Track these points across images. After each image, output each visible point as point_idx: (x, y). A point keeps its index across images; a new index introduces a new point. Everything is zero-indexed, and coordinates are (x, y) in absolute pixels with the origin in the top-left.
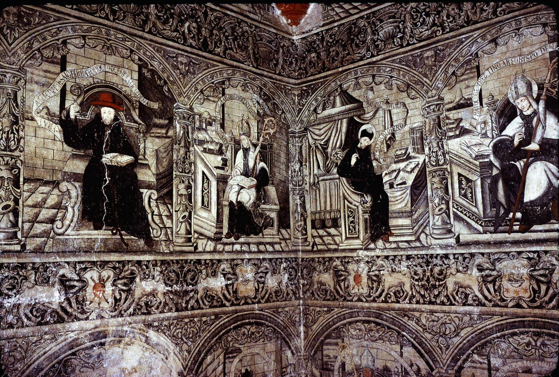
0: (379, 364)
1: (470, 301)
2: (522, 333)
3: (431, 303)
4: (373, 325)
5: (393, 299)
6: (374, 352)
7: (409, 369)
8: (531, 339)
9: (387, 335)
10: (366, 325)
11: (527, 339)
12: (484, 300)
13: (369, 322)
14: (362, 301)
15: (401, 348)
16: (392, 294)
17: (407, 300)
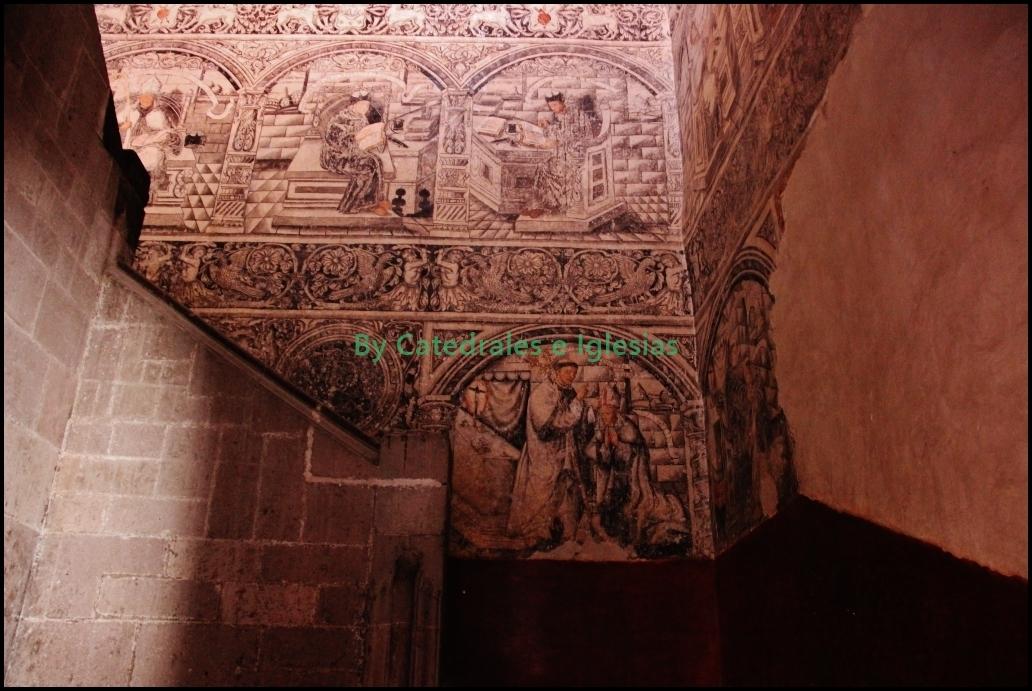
0: (167, 90)
1: (300, 29)
2: (348, 53)
3: (254, 32)
4: (170, 55)
5: (208, 29)
6: (162, 79)
7: (206, 89)
8: (355, 57)
9: (188, 62)
10: (160, 55)
11: (351, 56)
12: (315, 29)
13: (164, 52)
14: (163, 33)
15: (204, 72)
16: (207, 26)
17: (226, 31)
